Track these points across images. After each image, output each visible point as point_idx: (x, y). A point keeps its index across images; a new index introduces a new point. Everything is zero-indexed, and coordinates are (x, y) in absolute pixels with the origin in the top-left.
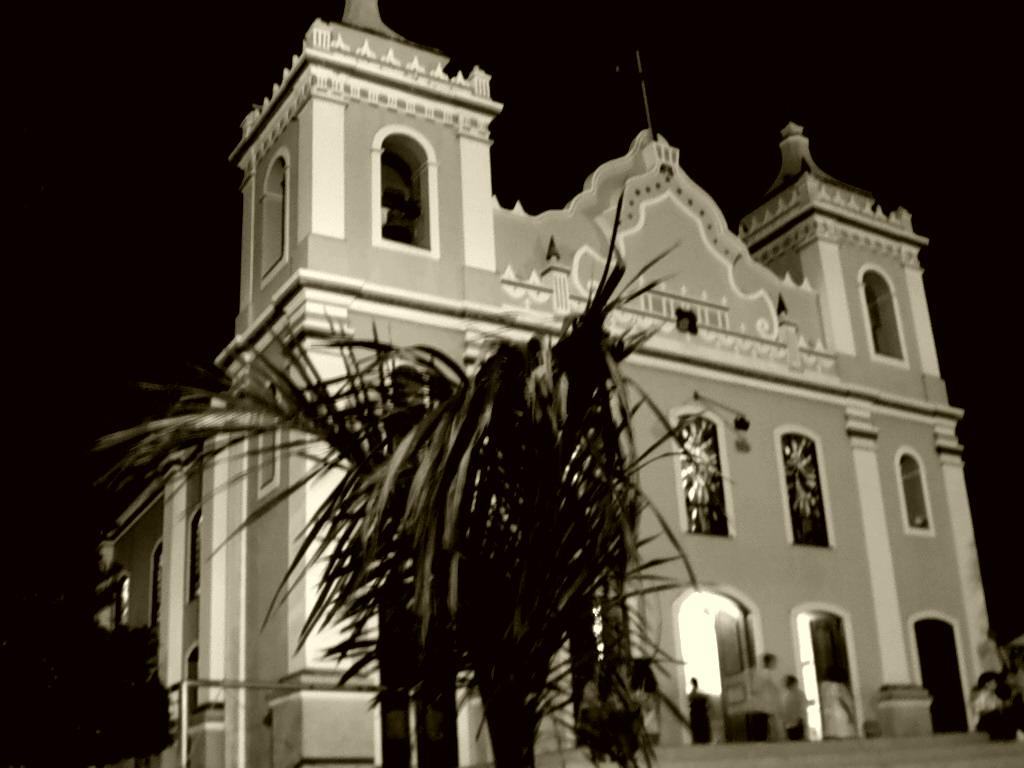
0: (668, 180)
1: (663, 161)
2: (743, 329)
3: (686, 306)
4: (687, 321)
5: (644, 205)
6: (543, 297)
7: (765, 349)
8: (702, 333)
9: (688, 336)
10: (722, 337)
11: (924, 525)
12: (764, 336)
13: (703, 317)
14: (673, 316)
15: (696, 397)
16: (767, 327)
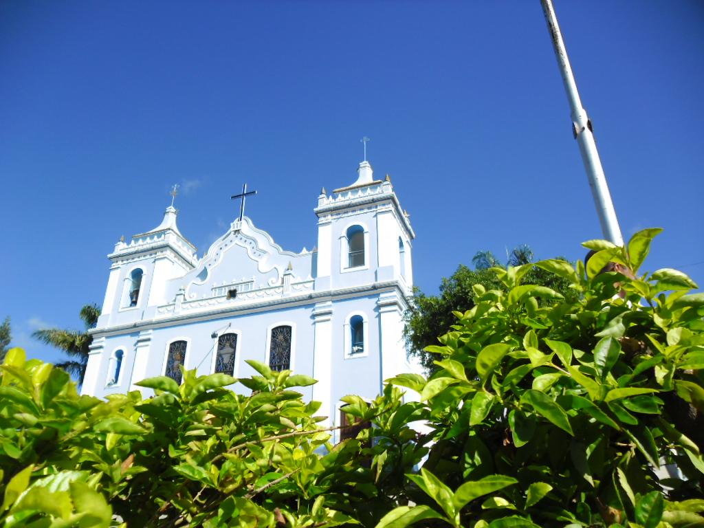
0: (237, 236)
1: (236, 229)
2: (262, 286)
3: (232, 289)
4: (233, 294)
5: (222, 253)
6: (172, 307)
7: (272, 291)
8: (239, 296)
9: (232, 300)
10: (248, 294)
11: (362, 351)
12: (273, 286)
13: (240, 289)
14: (226, 294)
15: (230, 326)
16: (274, 279)
